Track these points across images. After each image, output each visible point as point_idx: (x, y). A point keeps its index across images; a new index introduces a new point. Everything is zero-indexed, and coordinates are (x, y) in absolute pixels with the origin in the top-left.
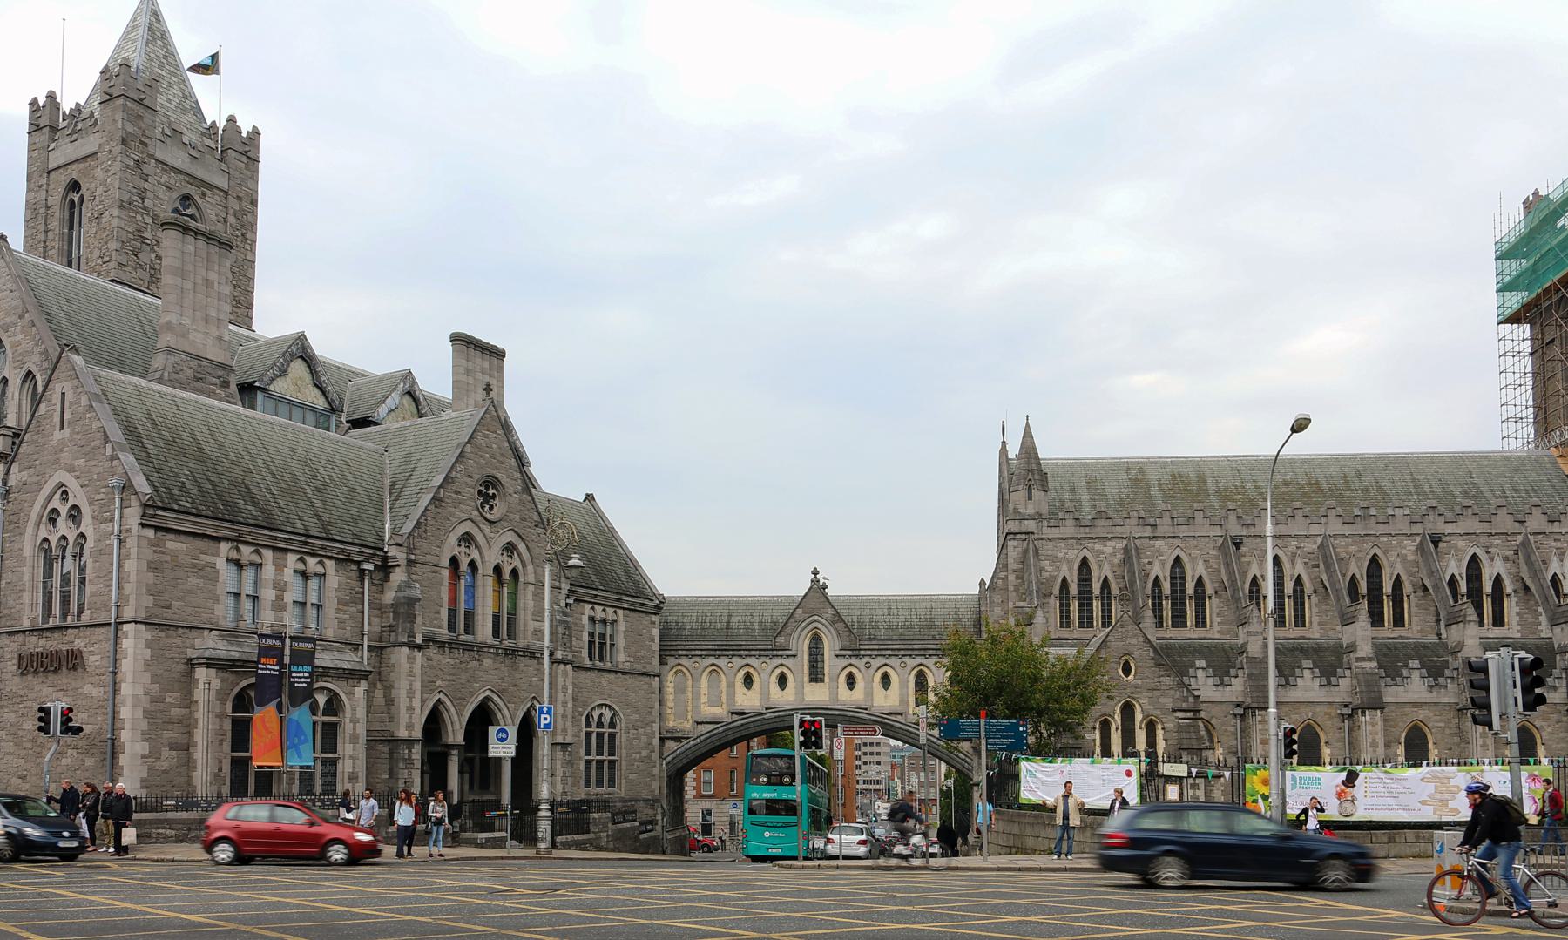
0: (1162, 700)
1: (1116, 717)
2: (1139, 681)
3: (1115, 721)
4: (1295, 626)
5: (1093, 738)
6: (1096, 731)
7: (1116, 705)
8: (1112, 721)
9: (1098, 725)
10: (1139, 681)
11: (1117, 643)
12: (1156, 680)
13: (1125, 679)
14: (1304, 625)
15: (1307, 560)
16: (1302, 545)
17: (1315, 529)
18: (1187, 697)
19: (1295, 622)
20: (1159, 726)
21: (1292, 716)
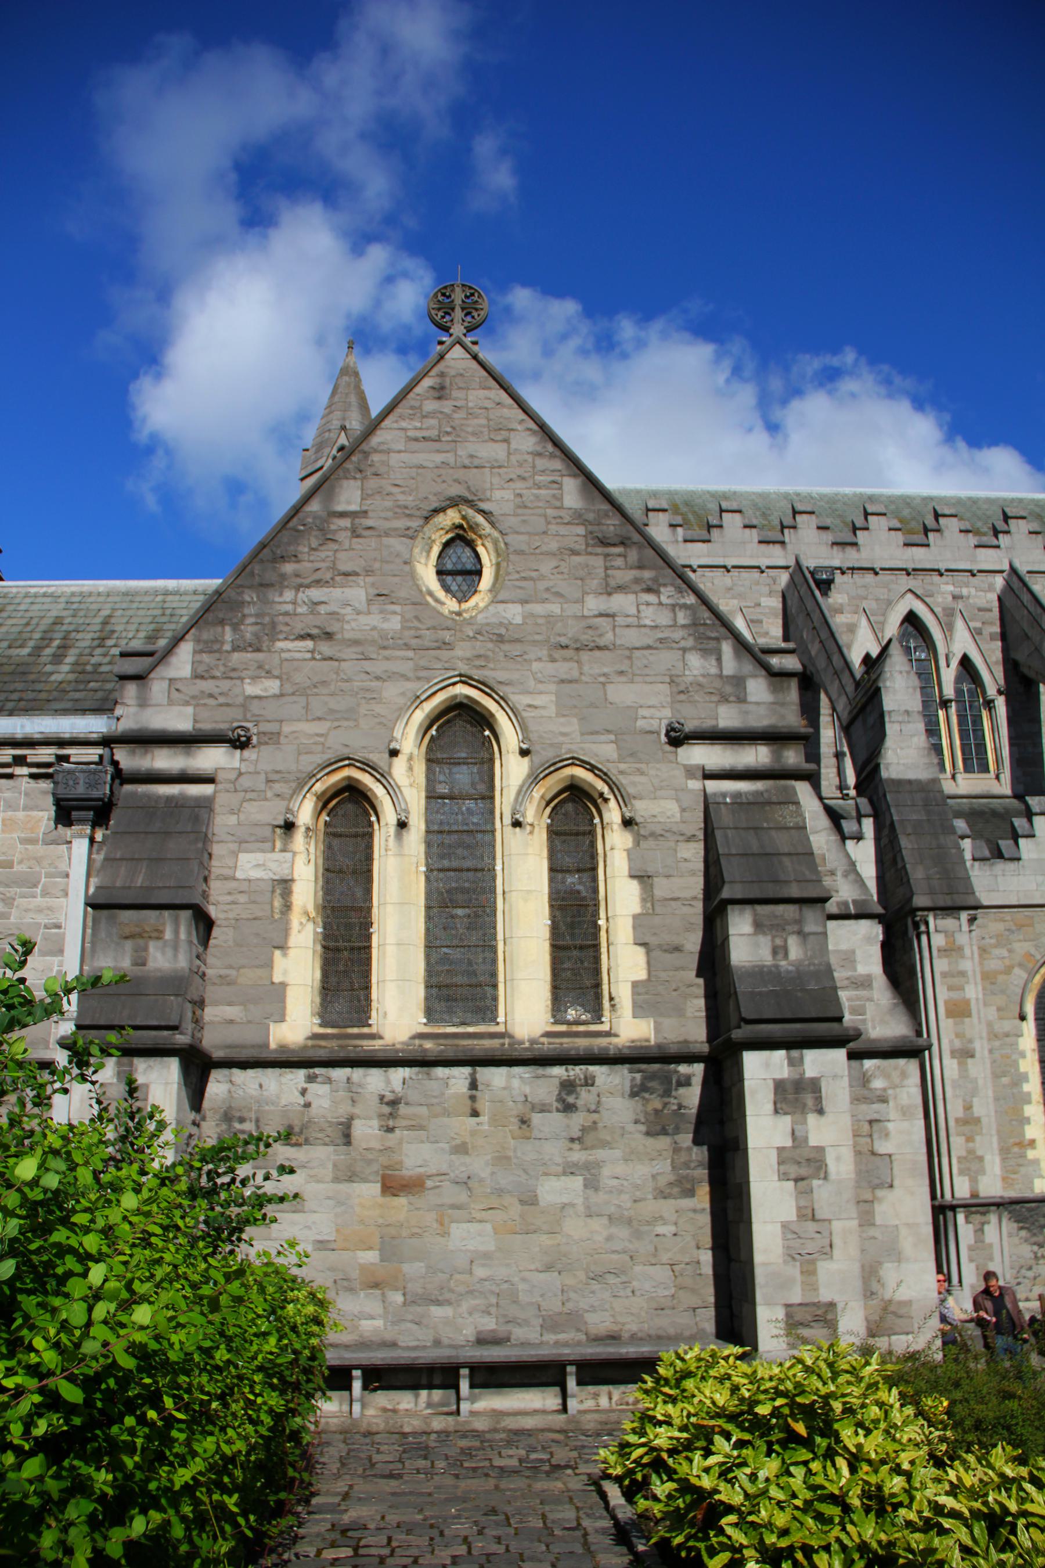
0: (621, 693)
1: (399, 768)
2: (514, 613)
3: (392, 790)
4: (968, 769)
5: (283, 872)
6: (299, 837)
7: (403, 711)
8: (379, 790)
9: (305, 812)
10: (514, 613)
11: (420, 458)
12: (593, 604)
13: (451, 604)
14: (985, 769)
15: (978, 625)
16: (965, 591)
17: (988, 559)
18: (739, 682)
19: (964, 760)
20: (613, 813)
21: (1017, 946)
